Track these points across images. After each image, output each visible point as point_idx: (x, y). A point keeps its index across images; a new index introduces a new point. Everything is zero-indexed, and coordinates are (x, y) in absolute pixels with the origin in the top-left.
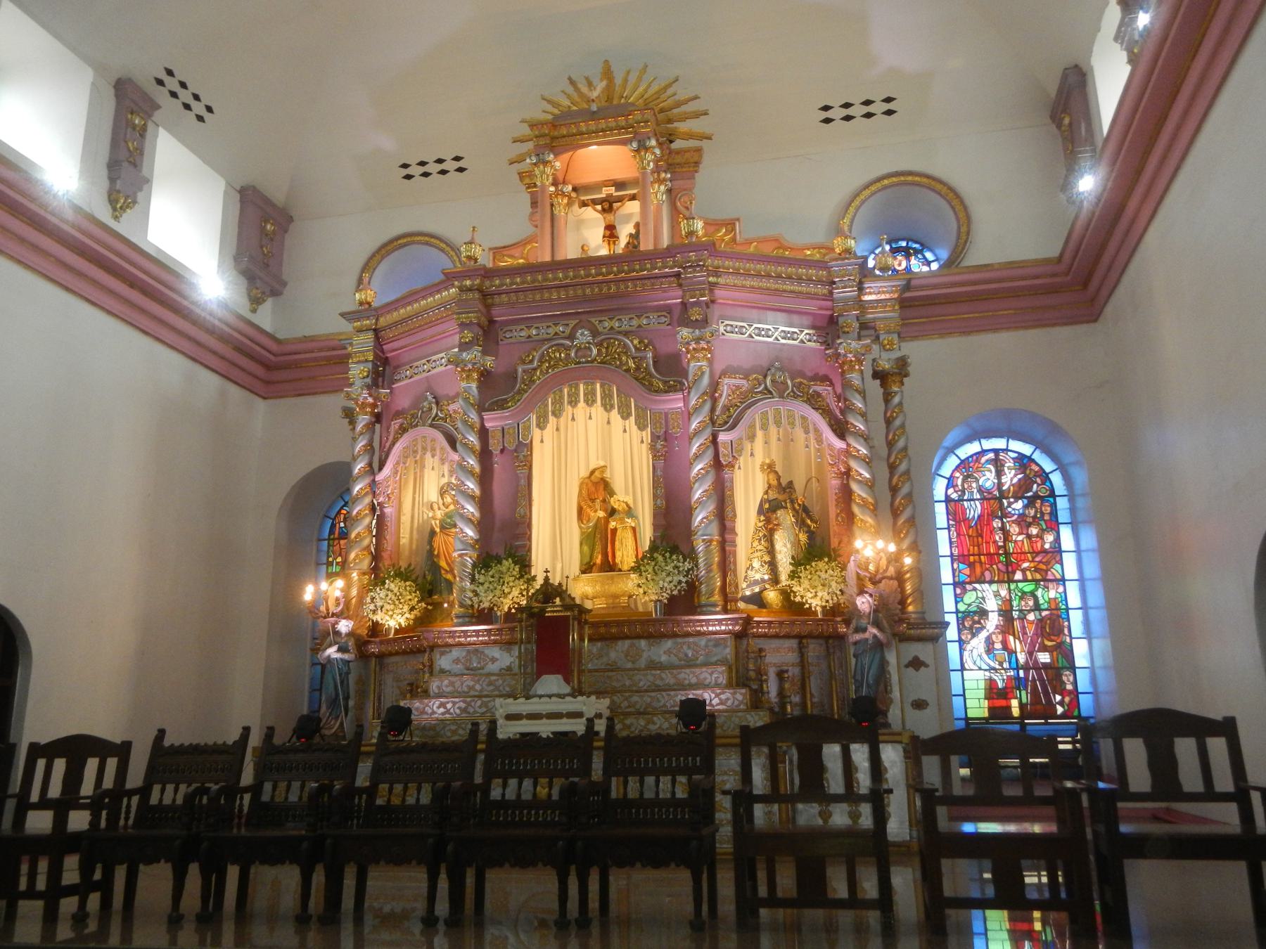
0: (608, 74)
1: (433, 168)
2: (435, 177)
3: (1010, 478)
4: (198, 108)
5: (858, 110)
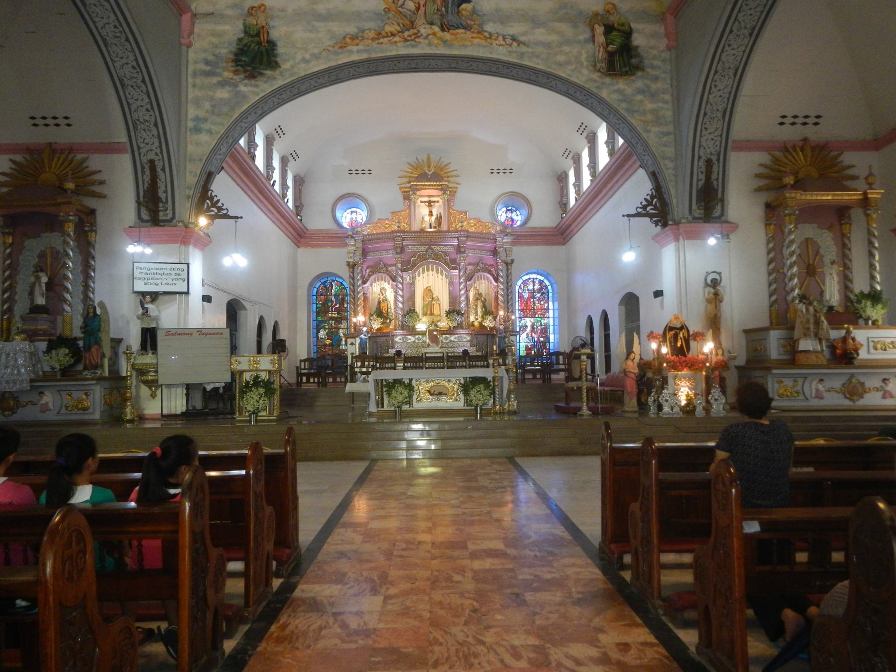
0: (429, 158)
2: (360, 175)
3: (537, 287)
4: (296, 158)
5: (502, 171)
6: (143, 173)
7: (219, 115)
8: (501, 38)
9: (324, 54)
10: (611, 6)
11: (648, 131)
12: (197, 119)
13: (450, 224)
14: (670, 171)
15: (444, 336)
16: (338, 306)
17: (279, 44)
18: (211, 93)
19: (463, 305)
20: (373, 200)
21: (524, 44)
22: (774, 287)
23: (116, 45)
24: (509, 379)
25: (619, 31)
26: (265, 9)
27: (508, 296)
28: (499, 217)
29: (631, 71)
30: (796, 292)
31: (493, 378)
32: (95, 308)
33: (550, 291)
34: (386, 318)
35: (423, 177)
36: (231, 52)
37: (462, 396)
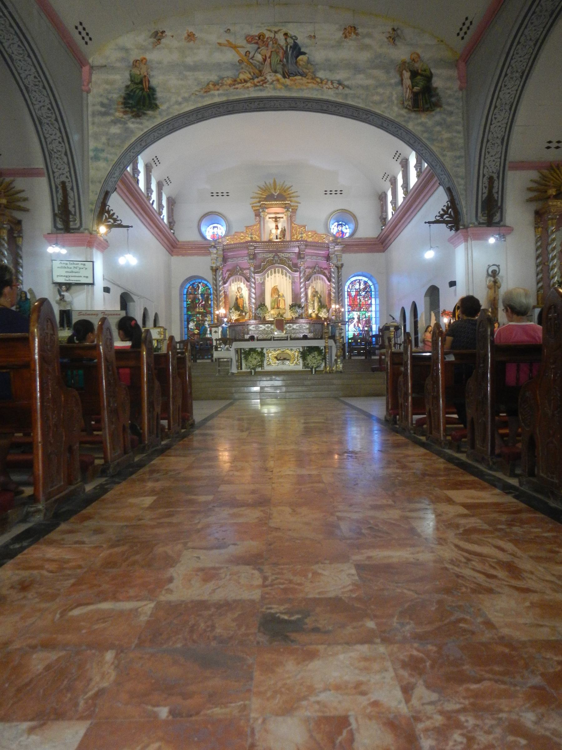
0: (275, 181)
1: (220, 194)
2: (220, 197)
3: (362, 286)
4: (169, 183)
6: (57, 192)
7: (113, 146)
8: (329, 82)
9: (193, 97)
10: (416, 56)
11: (444, 156)
12: (96, 150)
13: (292, 235)
14: (462, 187)
15: (288, 325)
16: (204, 303)
17: (158, 89)
18: (107, 130)
19: (303, 300)
20: (231, 217)
21: (348, 87)
22: (540, 276)
23: (35, 91)
24: (337, 348)
25: (422, 75)
26: (146, 61)
27: (339, 293)
28: (332, 231)
29: (431, 108)
30: (556, 278)
31: (325, 347)
32: (26, 293)
33: (373, 290)
34: (242, 311)
35: (271, 197)
36: (121, 96)
37: (301, 361)
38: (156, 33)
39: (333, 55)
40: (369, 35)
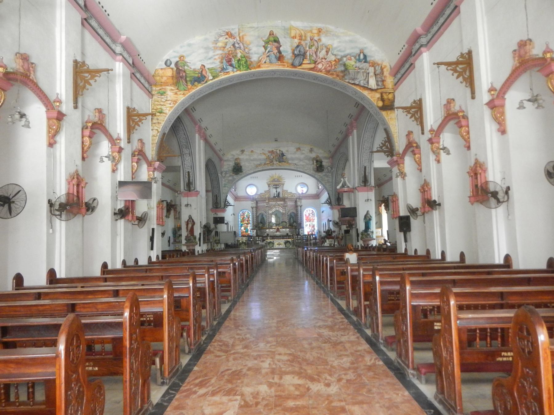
3: (311, 212)
12: (225, 184)
38: (242, 151)
39: (293, 156)
40: (303, 150)
